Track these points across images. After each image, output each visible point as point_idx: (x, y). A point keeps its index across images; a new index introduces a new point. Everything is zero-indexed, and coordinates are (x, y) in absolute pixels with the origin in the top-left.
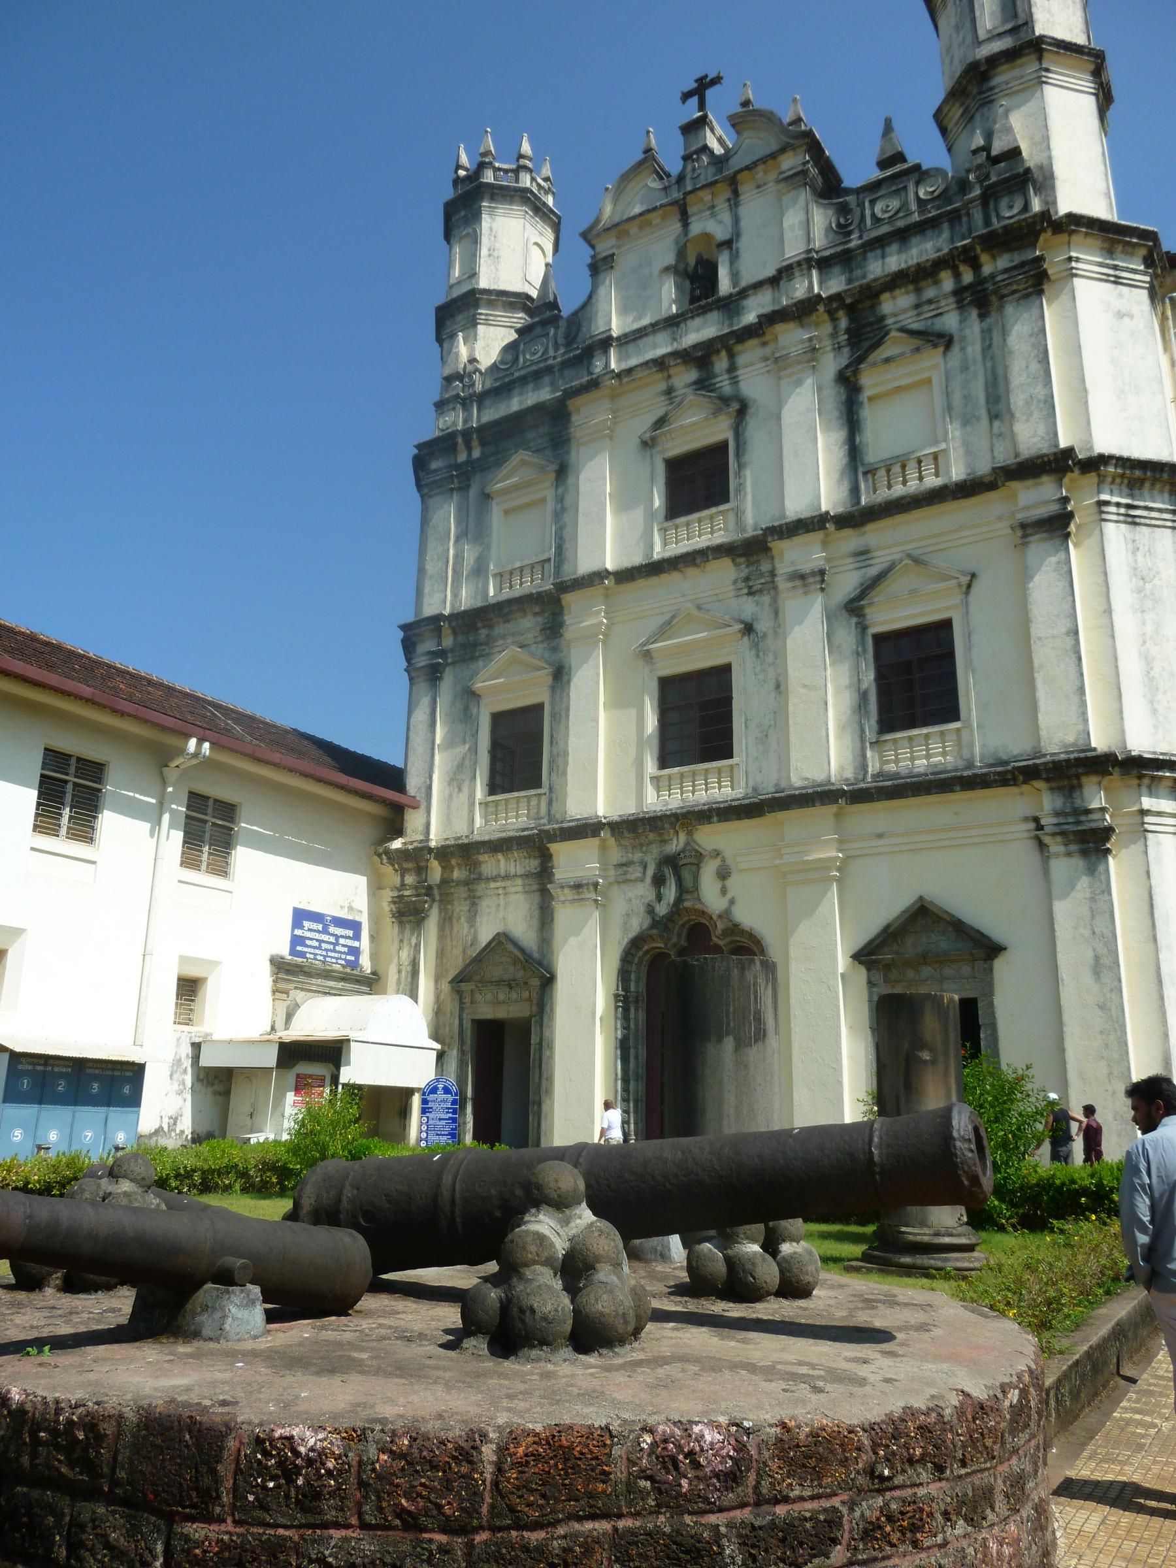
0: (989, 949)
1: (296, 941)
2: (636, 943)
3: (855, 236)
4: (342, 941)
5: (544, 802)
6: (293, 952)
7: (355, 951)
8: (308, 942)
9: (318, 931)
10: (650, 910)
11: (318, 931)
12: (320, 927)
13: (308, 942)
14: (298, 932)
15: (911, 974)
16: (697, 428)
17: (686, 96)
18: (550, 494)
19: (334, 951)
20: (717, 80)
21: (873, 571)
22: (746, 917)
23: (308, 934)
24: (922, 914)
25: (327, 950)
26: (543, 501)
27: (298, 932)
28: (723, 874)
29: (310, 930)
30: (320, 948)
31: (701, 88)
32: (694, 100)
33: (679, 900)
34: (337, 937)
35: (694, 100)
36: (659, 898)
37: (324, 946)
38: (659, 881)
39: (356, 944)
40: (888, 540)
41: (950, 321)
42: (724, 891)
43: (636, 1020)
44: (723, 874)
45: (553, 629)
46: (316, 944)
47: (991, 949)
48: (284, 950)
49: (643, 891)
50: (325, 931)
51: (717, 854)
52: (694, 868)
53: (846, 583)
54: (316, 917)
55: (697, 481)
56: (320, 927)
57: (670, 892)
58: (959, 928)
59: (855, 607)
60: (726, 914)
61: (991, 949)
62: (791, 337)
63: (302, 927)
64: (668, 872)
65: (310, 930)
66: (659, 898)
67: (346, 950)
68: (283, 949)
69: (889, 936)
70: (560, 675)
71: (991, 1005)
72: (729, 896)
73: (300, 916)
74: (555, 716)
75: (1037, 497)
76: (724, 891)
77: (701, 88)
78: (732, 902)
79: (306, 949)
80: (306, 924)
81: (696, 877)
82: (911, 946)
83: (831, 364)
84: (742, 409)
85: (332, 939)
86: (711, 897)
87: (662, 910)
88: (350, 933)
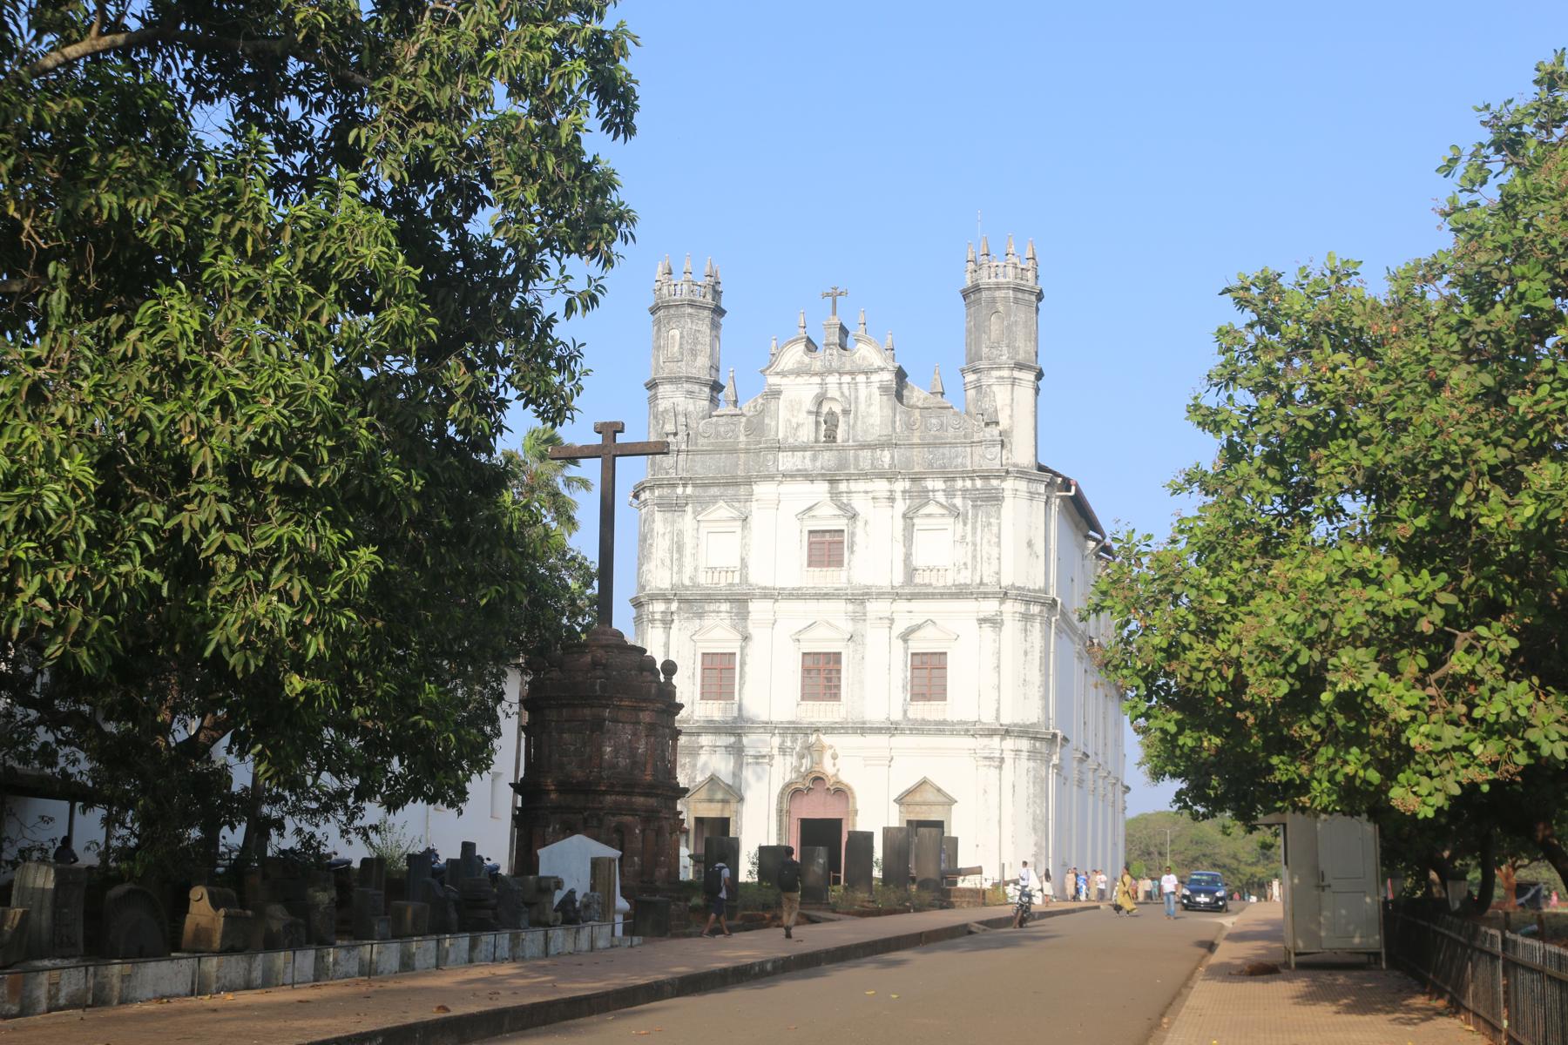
0: (952, 802)
2: (788, 785)
3: (917, 434)
16: (826, 517)
18: (739, 530)
22: (846, 778)
24: (924, 782)
28: (834, 757)
38: (802, 757)
40: (922, 609)
41: (958, 501)
44: (834, 757)
45: (743, 615)
47: (952, 802)
49: (791, 760)
53: (900, 627)
55: (826, 548)
58: (939, 790)
59: (905, 637)
62: (881, 486)
69: (909, 792)
70: (746, 638)
74: (743, 664)
75: (990, 607)
82: (917, 798)
83: (901, 506)
84: (854, 517)
86: (828, 768)
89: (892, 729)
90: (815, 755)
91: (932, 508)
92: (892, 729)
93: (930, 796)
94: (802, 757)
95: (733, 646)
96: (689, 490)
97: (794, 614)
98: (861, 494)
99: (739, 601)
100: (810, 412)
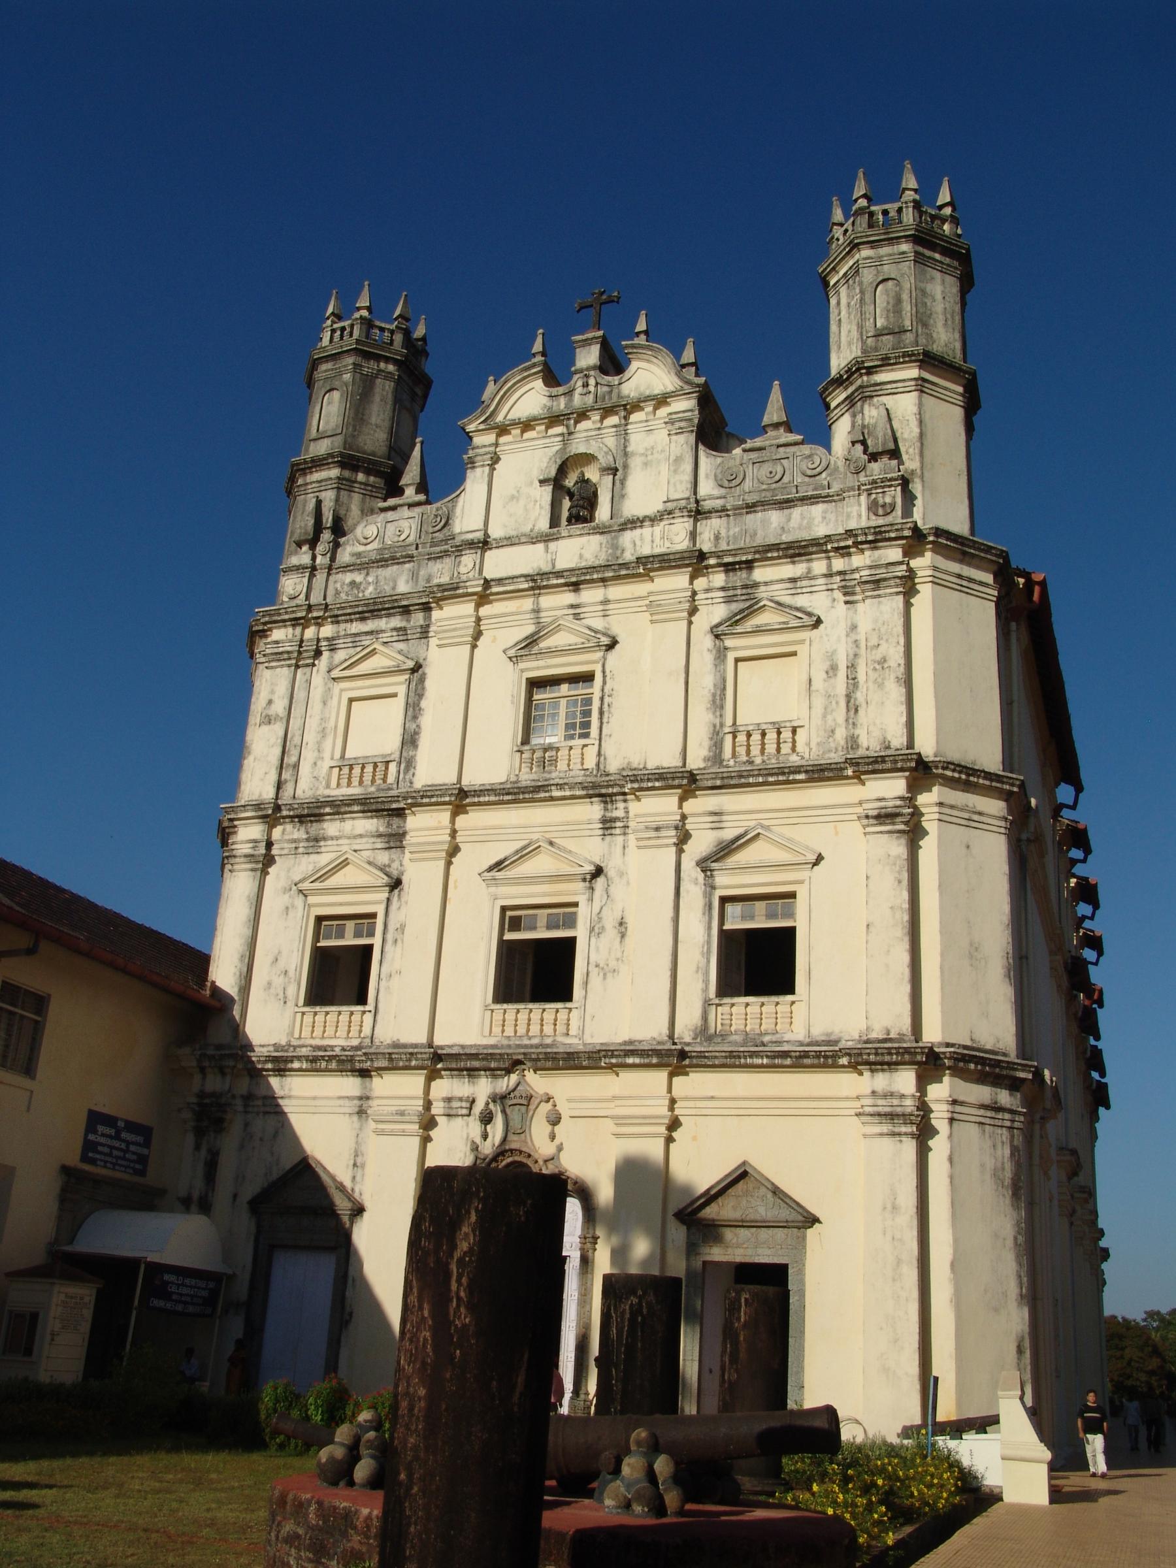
1: (89, 1147)
4: (132, 1148)
5: (368, 1018)
6: (84, 1158)
7: (143, 1160)
8: (100, 1148)
9: (110, 1137)
10: (475, 1148)
11: (110, 1137)
12: (113, 1132)
13: (100, 1148)
14: (91, 1137)
18: (402, 690)
19: (124, 1158)
21: (729, 834)
23: (102, 1140)
25: (117, 1158)
26: (395, 695)
27: (91, 1137)
29: (103, 1135)
30: (110, 1155)
33: (504, 1140)
34: (128, 1143)
36: (485, 1136)
37: (115, 1153)
38: (487, 1119)
39: (145, 1151)
42: (553, 1137)
44: (555, 1120)
45: (395, 840)
46: (106, 1150)
48: (73, 1158)
50: (117, 1137)
52: (523, 1108)
53: (702, 843)
54: (109, 1120)
56: (113, 1132)
57: (497, 1130)
59: (706, 865)
63: (95, 1132)
64: (496, 1109)
65: (103, 1135)
66: (485, 1136)
67: (135, 1157)
68: (73, 1158)
71: (801, 1272)
72: (557, 1141)
73: (95, 1119)
76: (553, 1137)
78: (560, 1148)
79: (98, 1156)
80: (100, 1128)
81: (526, 1120)
85: (123, 1146)
87: (488, 1149)
88: (140, 1139)
89: (676, 1059)
90: (515, 1115)
91: (765, 618)
92: (676, 1059)
94: (487, 1119)
95: (373, 902)
96: (327, 631)
97: (492, 830)
98: (625, 608)
99: (390, 810)
100: (542, 482)
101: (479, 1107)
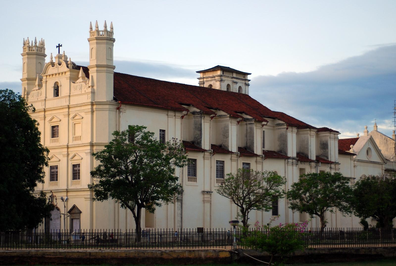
15: (74, 215)
17: (57, 47)
20: (61, 46)
31: (59, 46)
32: (58, 48)
35: (58, 48)
42: (56, 202)
43: (47, 220)
44: (56, 199)
47: (81, 212)
51: (55, 196)
60: (56, 205)
61: (81, 212)
64: (50, 198)
69: (71, 210)
77: (59, 46)
78: (57, 203)
93: (77, 211)
101: (49, 198)
